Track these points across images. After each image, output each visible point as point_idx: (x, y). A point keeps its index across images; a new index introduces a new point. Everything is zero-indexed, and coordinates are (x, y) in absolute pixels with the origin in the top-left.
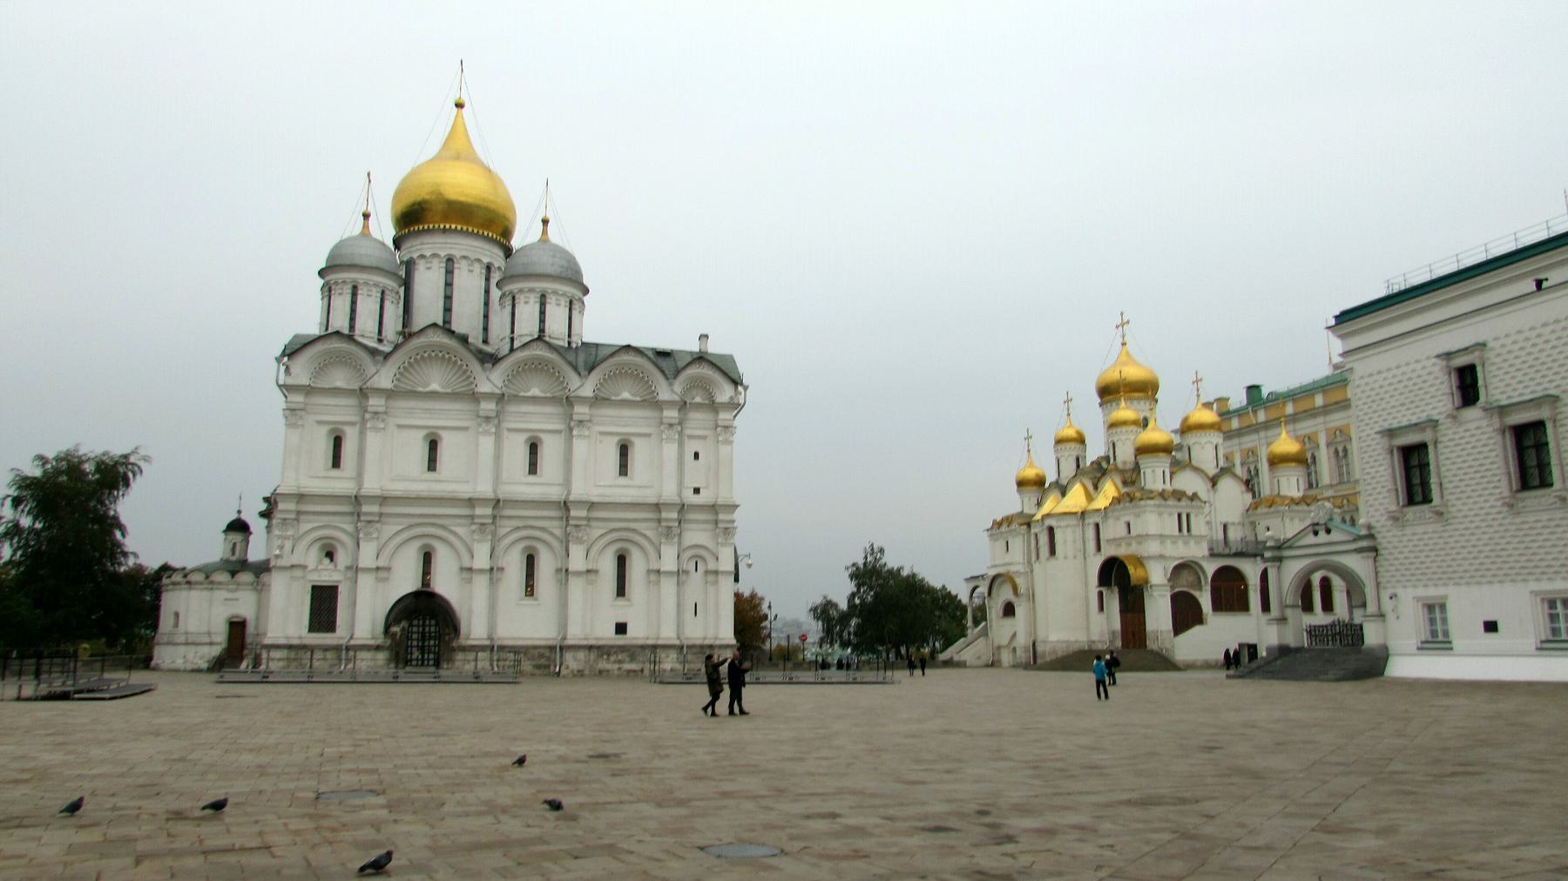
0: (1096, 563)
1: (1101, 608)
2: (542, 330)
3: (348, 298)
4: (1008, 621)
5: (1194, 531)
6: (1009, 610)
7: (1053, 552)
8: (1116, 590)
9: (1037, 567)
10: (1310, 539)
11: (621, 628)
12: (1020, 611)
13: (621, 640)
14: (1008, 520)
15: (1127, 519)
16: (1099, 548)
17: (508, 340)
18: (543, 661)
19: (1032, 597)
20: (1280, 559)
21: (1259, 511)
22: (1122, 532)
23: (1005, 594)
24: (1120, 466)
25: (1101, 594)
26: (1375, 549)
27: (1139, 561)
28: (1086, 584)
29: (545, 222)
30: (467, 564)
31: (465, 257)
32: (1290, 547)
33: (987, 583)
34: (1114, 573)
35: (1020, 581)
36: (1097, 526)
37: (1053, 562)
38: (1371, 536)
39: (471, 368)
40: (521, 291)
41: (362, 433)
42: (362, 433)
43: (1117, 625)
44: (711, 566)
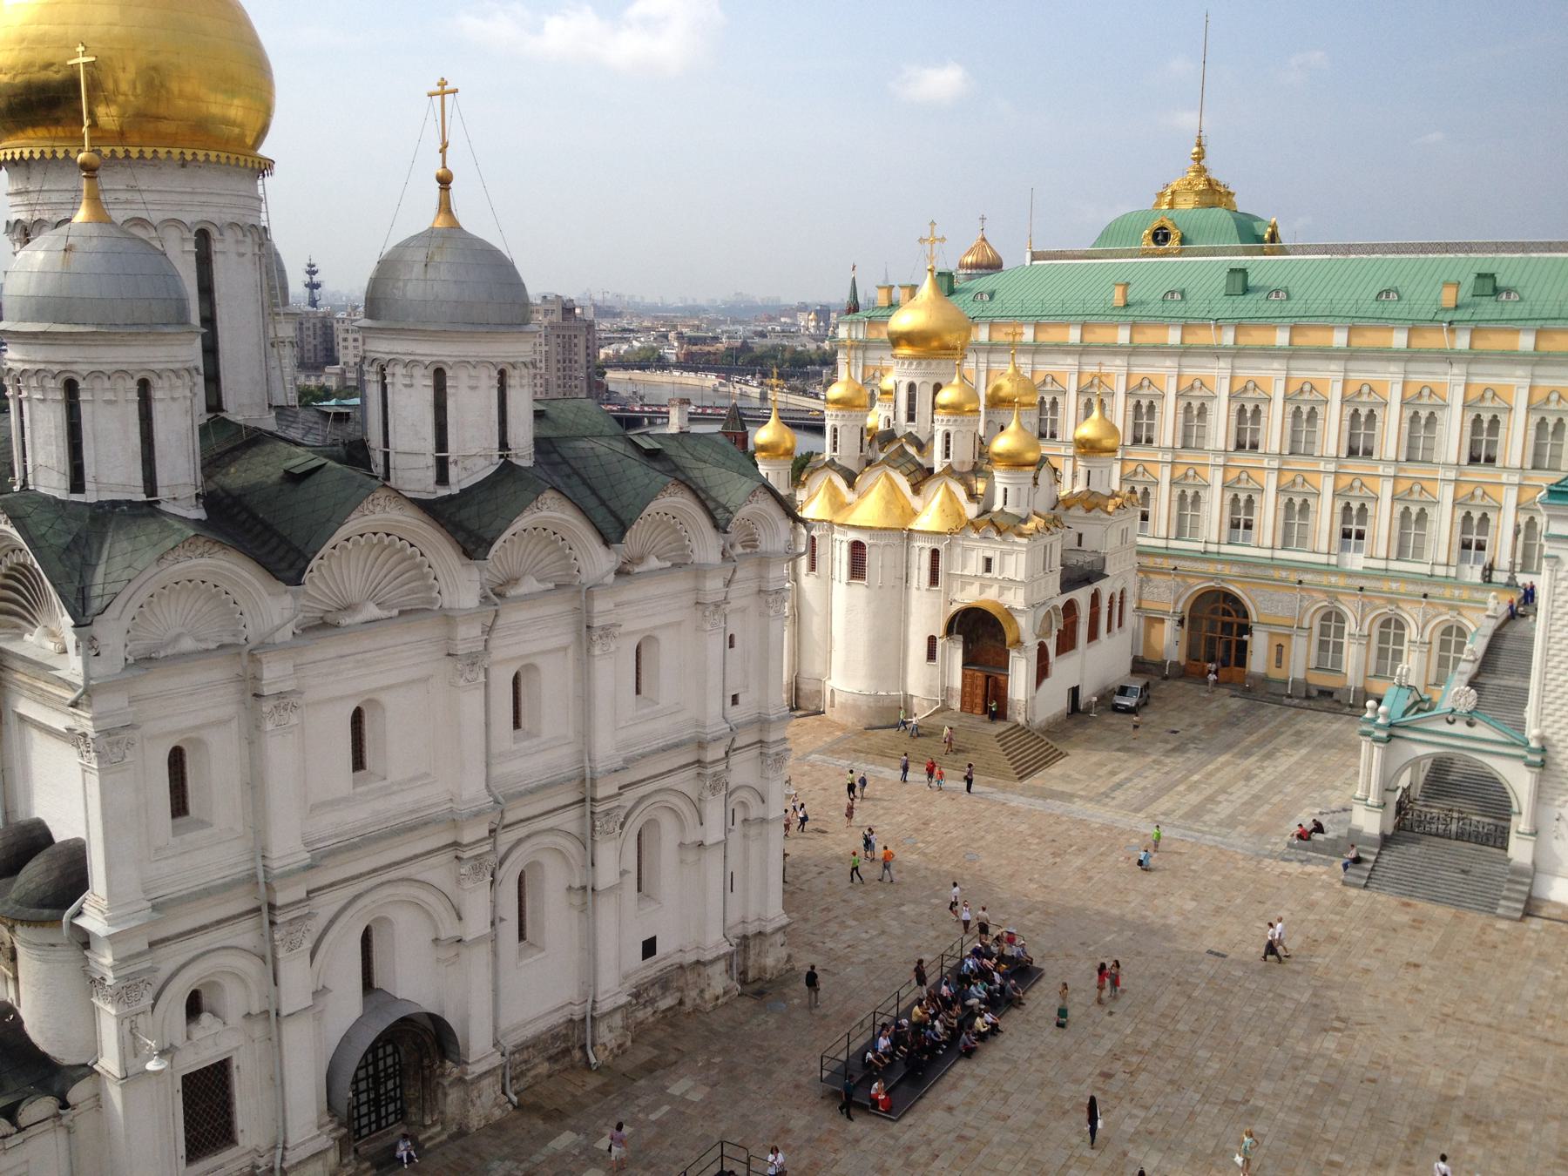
1: (931, 655)
2: (504, 445)
3: (133, 411)
8: (961, 637)
10: (1444, 727)
11: (649, 948)
13: (653, 967)
15: (989, 554)
16: (934, 580)
17: (431, 461)
18: (560, 1045)
20: (1391, 737)
21: (1071, 512)
22: (975, 566)
25: (932, 640)
26: (1543, 765)
27: (1009, 613)
29: (445, 181)
30: (449, 929)
31: (233, 225)
36: (935, 553)
38: (1543, 750)
39: (431, 557)
40: (464, 363)
41: (253, 737)
42: (253, 737)
43: (957, 682)
44: (755, 812)
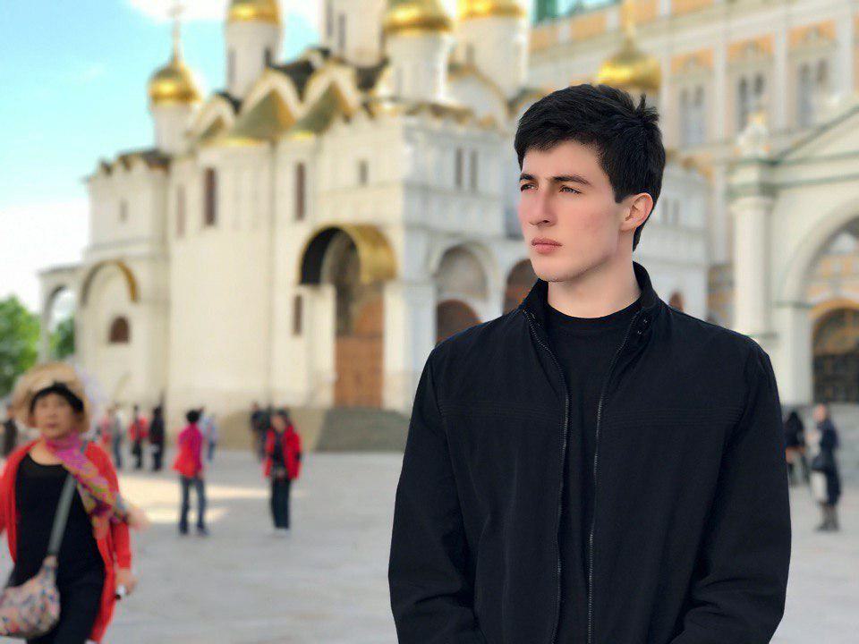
0: (293, 240)
4: (120, 350)
5: (481, 185)
6: (120, 331)
7: (210, 216)
9: (178, 250)
12: (138, 330)
14: (126, 160)
16: (300, 211)
19: (162, 304)
23: (112, 299)
24: (351, 52)
28: (271, 283)
32: (803, 161)
33: (81, 276)
34: (329, 256)
35: (142, 274)
37: (211, 233)
